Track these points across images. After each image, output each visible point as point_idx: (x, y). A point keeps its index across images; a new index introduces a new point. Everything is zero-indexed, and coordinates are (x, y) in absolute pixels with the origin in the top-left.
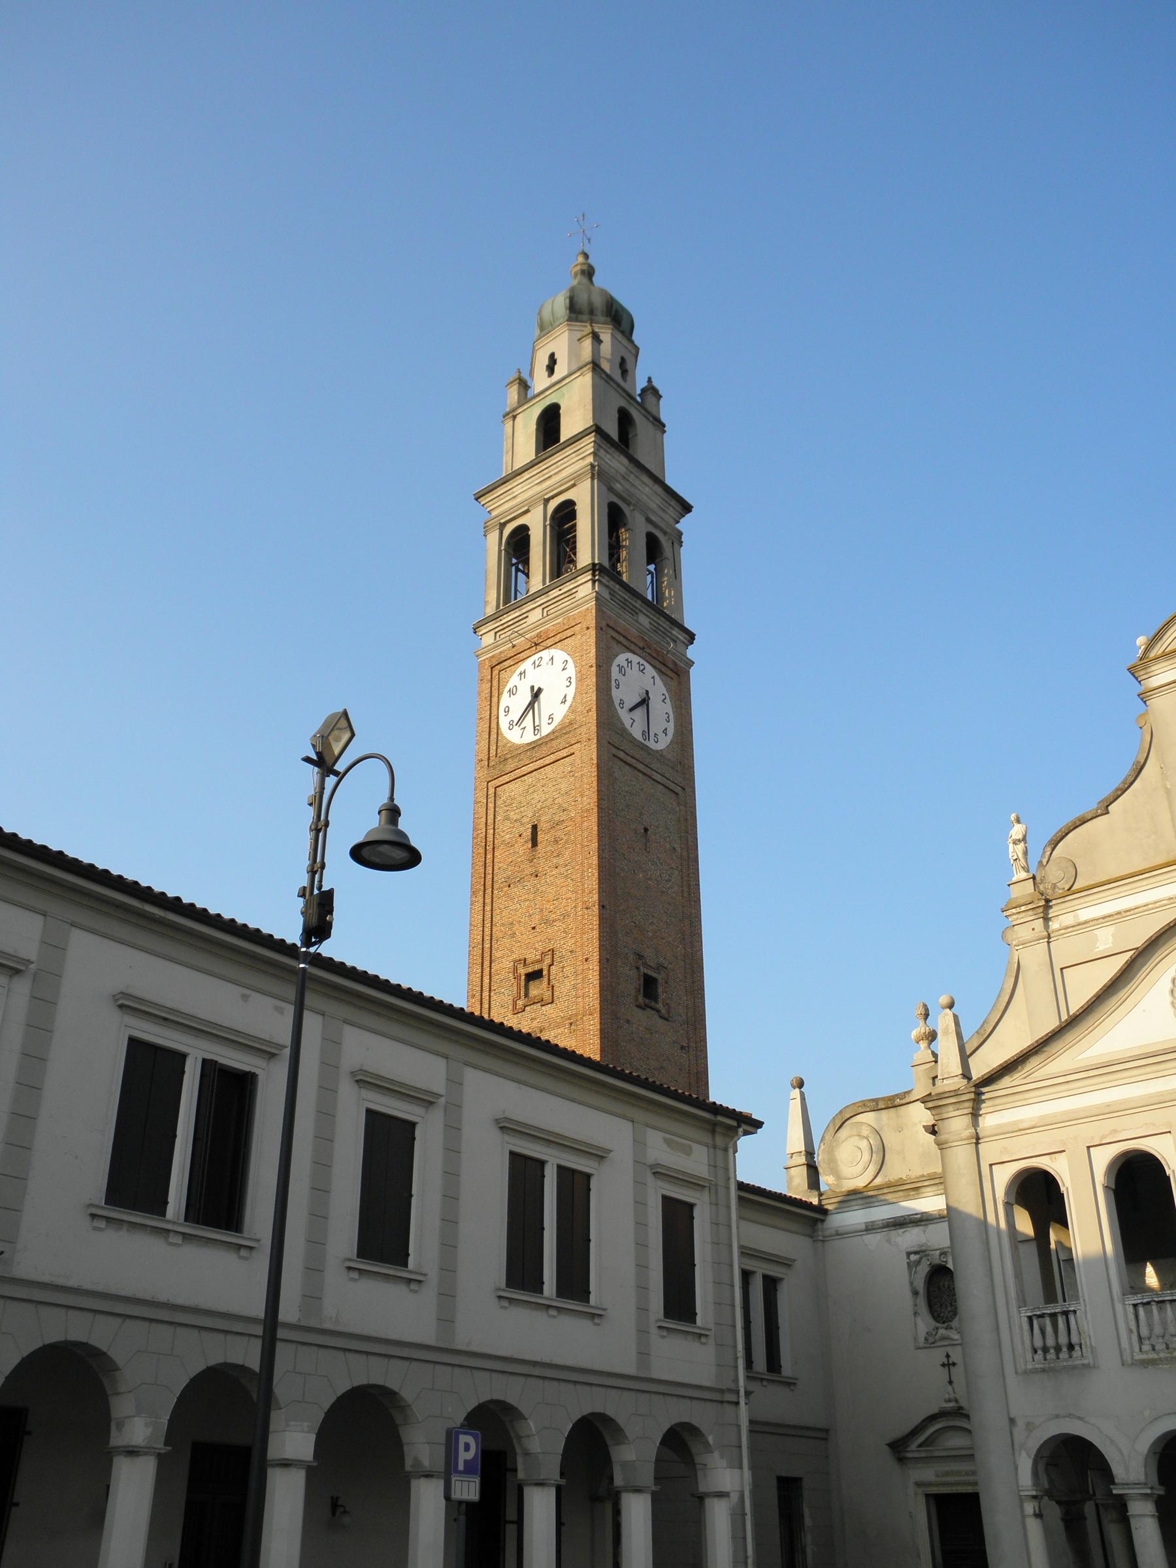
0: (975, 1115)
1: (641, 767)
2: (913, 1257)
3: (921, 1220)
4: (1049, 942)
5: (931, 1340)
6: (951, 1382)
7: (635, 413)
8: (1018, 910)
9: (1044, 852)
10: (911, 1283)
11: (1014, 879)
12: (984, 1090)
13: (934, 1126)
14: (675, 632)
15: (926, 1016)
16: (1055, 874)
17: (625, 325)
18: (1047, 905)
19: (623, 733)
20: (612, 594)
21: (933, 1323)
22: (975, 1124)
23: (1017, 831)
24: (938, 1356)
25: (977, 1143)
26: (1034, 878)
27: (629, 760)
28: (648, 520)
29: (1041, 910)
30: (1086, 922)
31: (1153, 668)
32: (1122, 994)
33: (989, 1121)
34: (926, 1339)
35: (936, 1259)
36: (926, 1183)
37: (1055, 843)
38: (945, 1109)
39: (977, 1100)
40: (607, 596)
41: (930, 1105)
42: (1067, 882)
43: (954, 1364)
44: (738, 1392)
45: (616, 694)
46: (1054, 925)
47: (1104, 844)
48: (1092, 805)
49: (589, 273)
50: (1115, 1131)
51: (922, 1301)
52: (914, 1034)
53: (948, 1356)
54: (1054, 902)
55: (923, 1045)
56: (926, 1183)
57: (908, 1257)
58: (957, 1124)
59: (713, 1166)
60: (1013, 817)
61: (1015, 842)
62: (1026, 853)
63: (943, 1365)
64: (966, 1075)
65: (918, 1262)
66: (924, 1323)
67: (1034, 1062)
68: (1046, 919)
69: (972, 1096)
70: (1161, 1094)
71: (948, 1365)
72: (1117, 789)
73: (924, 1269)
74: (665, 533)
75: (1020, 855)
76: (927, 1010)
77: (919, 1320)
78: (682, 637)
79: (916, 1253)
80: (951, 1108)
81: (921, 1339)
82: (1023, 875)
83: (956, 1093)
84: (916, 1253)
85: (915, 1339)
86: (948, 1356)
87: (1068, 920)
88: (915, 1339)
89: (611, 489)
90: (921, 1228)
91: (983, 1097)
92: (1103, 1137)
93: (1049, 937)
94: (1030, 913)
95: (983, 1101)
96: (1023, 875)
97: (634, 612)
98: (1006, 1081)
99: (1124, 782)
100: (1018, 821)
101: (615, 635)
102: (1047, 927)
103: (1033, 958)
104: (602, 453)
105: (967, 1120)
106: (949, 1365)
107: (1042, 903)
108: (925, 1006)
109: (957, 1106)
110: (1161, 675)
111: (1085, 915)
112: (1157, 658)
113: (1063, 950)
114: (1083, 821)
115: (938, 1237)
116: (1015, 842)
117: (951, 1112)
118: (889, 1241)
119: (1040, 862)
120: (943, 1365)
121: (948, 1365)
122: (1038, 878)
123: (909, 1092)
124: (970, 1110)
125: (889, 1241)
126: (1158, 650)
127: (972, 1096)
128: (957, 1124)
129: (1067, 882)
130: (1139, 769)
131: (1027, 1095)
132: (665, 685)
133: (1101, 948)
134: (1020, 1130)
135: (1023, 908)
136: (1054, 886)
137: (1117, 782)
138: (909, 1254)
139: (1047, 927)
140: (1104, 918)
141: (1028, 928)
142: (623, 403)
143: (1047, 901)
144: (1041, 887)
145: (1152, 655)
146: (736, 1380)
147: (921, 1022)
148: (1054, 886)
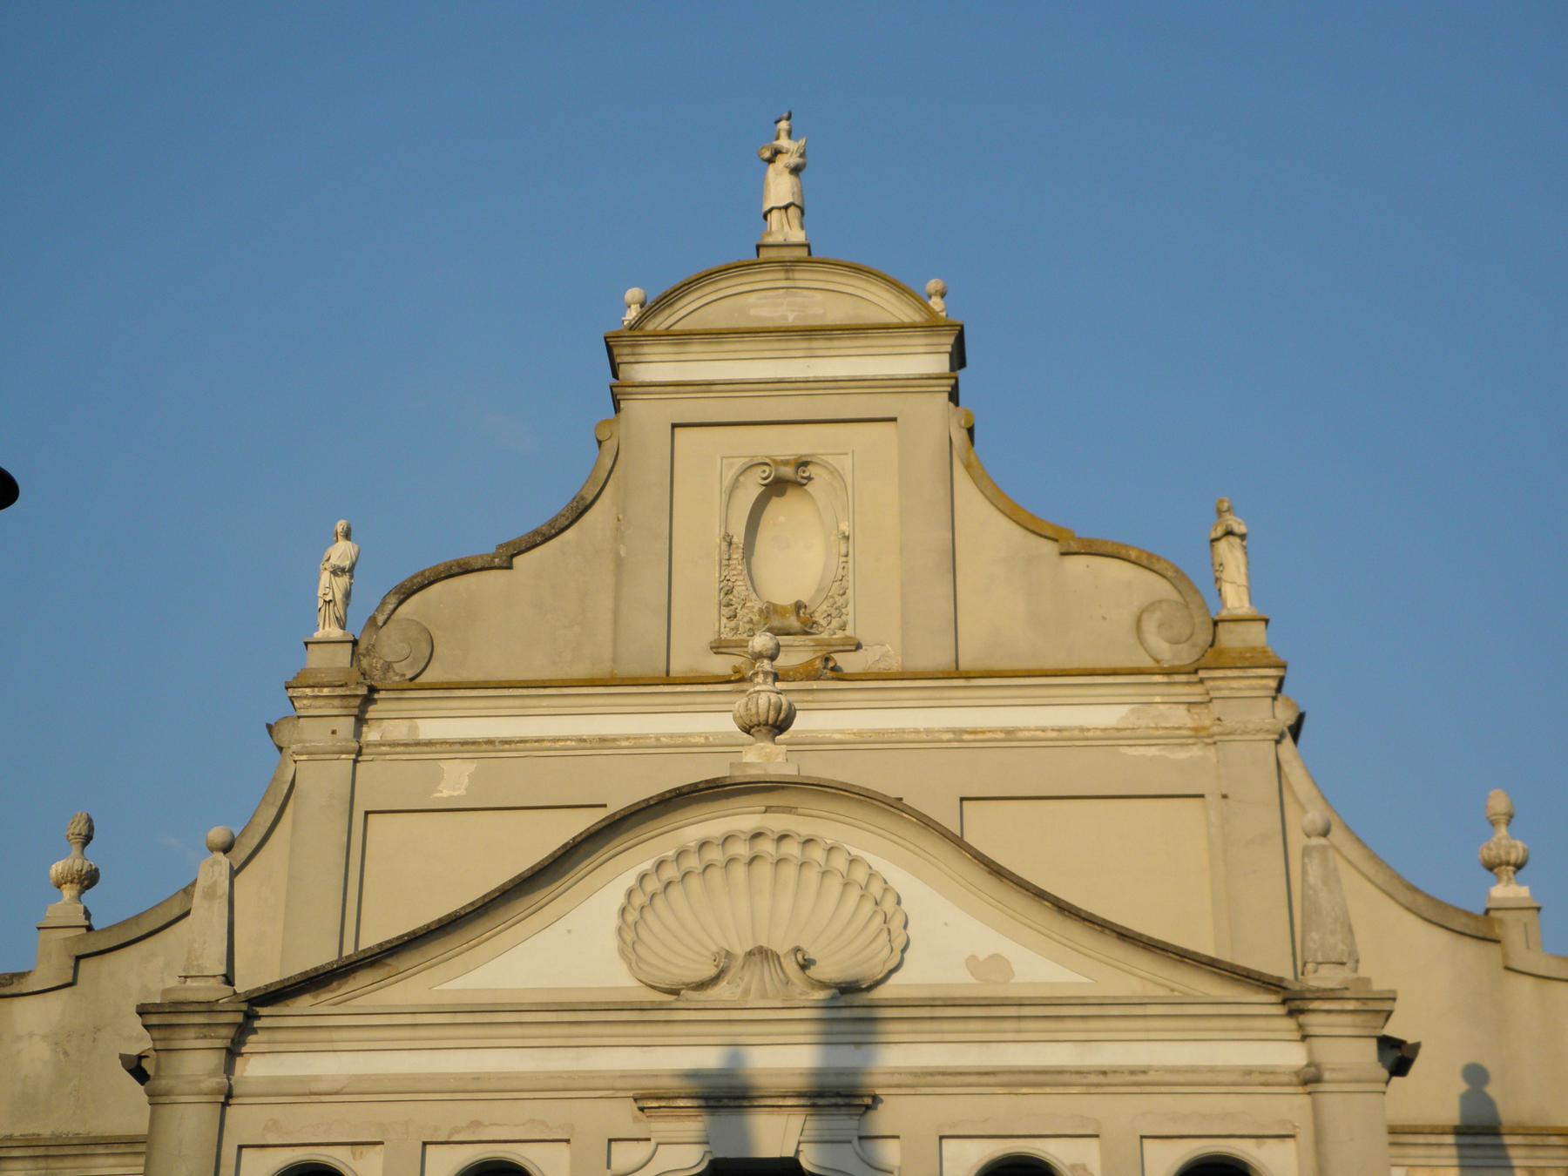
0: (233, 1053)
4: (356, 761)
8: (316, 692)
9: (383, 603)
11: (318, 635)
12: (262, 1011)
13: (140, 1057)
15: (88, 839)
16: (392, 646)
18: (368, 700)
22: (229, 1069)
23: (341, 553)
25: (225, 1104)
26: (355, 643)
29: (357, 702)
30: (429, 743)
31: (646, 350)
32: (541, 895)
33: (255, 1068)
36: (16, 1153)
37: (406, 592)
38: (178, 1033)
39: (244, 1029)
41: (154, 1020)
42: (411, 666)
46: (371, 734)
47: (491, 618)
48: (485, 547)
50: (477, 1124)
52: (57, 868)
54: (383, 694)
55: (68, 892)
56: (16, 1153)
58: (196, 1063)
60: (340, 526)
61: (337, 571)
62: (347, 595)
64: (229, 979)
67: (363, 978)
68: (361, 720)
69: (239, 1018)
70: (570, 1075)
72: (537, 532)
75: (339, 596)
76: (91, 829)
80: (192, 1033)
82: (335, 632)
83: (210, 1007)
87: (398, 730)
91: (257, 1024)
92: (456, 1130)
93: (359, 752)
94: (336, 702)
95: (255, 1031)
96: (335, 632)
98: (304, 1003)
99: (551, 524)
100: (347, 536)
102: (358, 734)
103: (321, 782)
105: (215, 1060)
107: (363, 691)
108: (89, 821)
109: (205, 1031)
110: (655, 366)
111: (430, 729)
112: (657, 336)
113: (380, 781)
114: (464, 569)
116: (337, 571)
117: (190, 1040)
119: (373, 619)
122: (362, 646)
123: (21, 976)
124: (227, 1043)
126: (659, 323)
127: (239, 1018)
128: (196, 1063)
129: (411, 666)
130: (579, 510)
131: (336, 1035)
133: (446, 793)
134: (308, 1093)
135: (326, 691)
136: (388, 666)
137: (538, 519)
139: (358, 734)
140: (464, 743)
141: (324, 726)
143: (373, 690)
144: (365, 663)
145: (650, 326)
147: (75, 850)
148: (388, 666)
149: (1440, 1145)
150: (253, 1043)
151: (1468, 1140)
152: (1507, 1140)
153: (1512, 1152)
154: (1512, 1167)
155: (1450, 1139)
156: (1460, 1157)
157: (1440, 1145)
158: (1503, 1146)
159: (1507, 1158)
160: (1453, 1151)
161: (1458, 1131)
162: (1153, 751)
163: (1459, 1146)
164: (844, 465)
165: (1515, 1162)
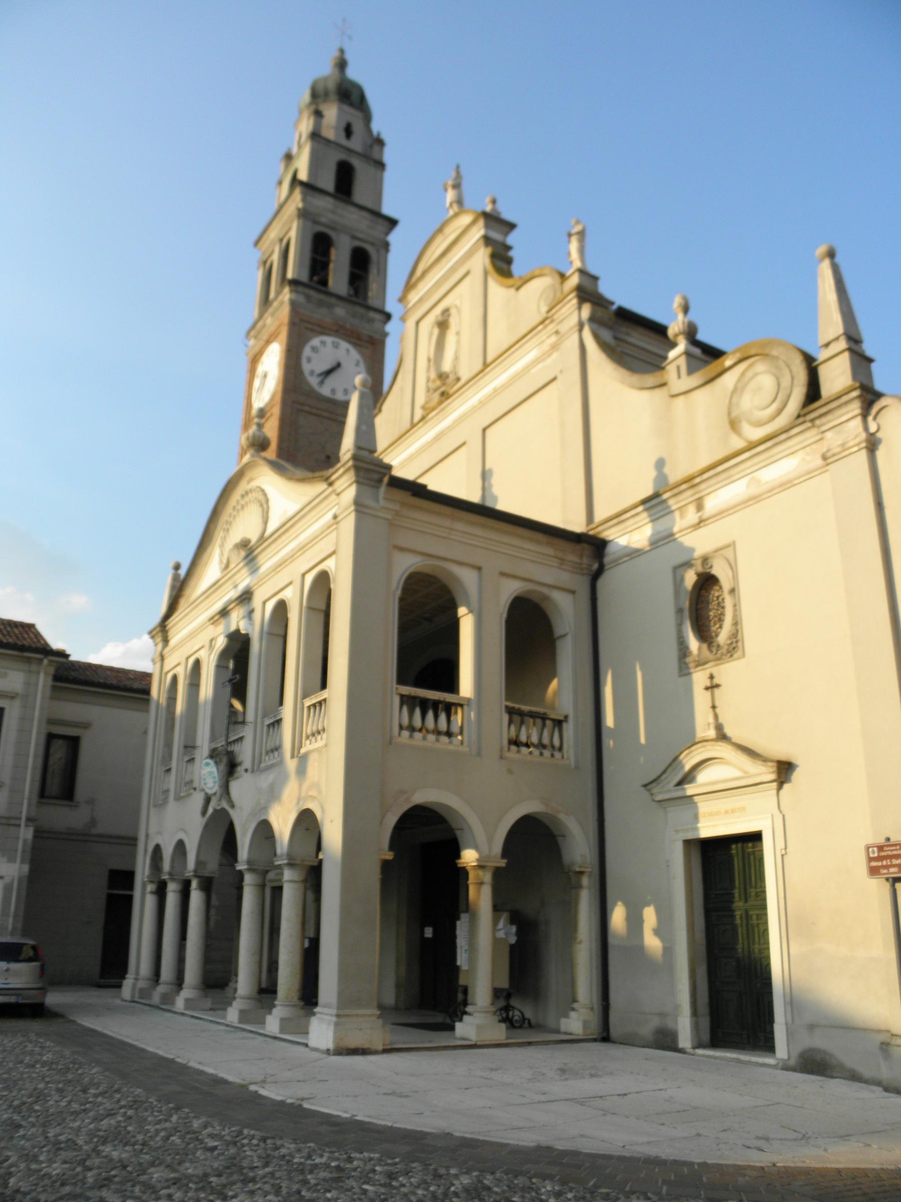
1: (326, 414)
7: (356, 162)
14: (372, 314)
17: (355, 97)
19: (312, 394)
20: (308, 298)
27: (314, 411)
28: (354, 237)
40: (301, 299)
44: (20, 819)
45: (306, 367)
49: (342, 64)
59: (27, 684)
74: (373, 244)
78: (378, 316)
89: (316, 222)
97: (330, 306)
101: (310, 326)
104: (309, 198)
132: (361, 353)
142: (342, 156)
146: (21, 812)
149: (637, 514)
150: (171, 634)
151: (648, 505)
152: (665, 496)
153: (671, 502)
154: (672, 512)
155: (641, 508)
156: (650, 516)
157: (637, 514)
158: (665, 501)
159: (669, 507)
160: (645, 515)
161: (644, 502)
162: (540, 366)
163: (646, 510)
164: (458, 303)
165: (674, 508)
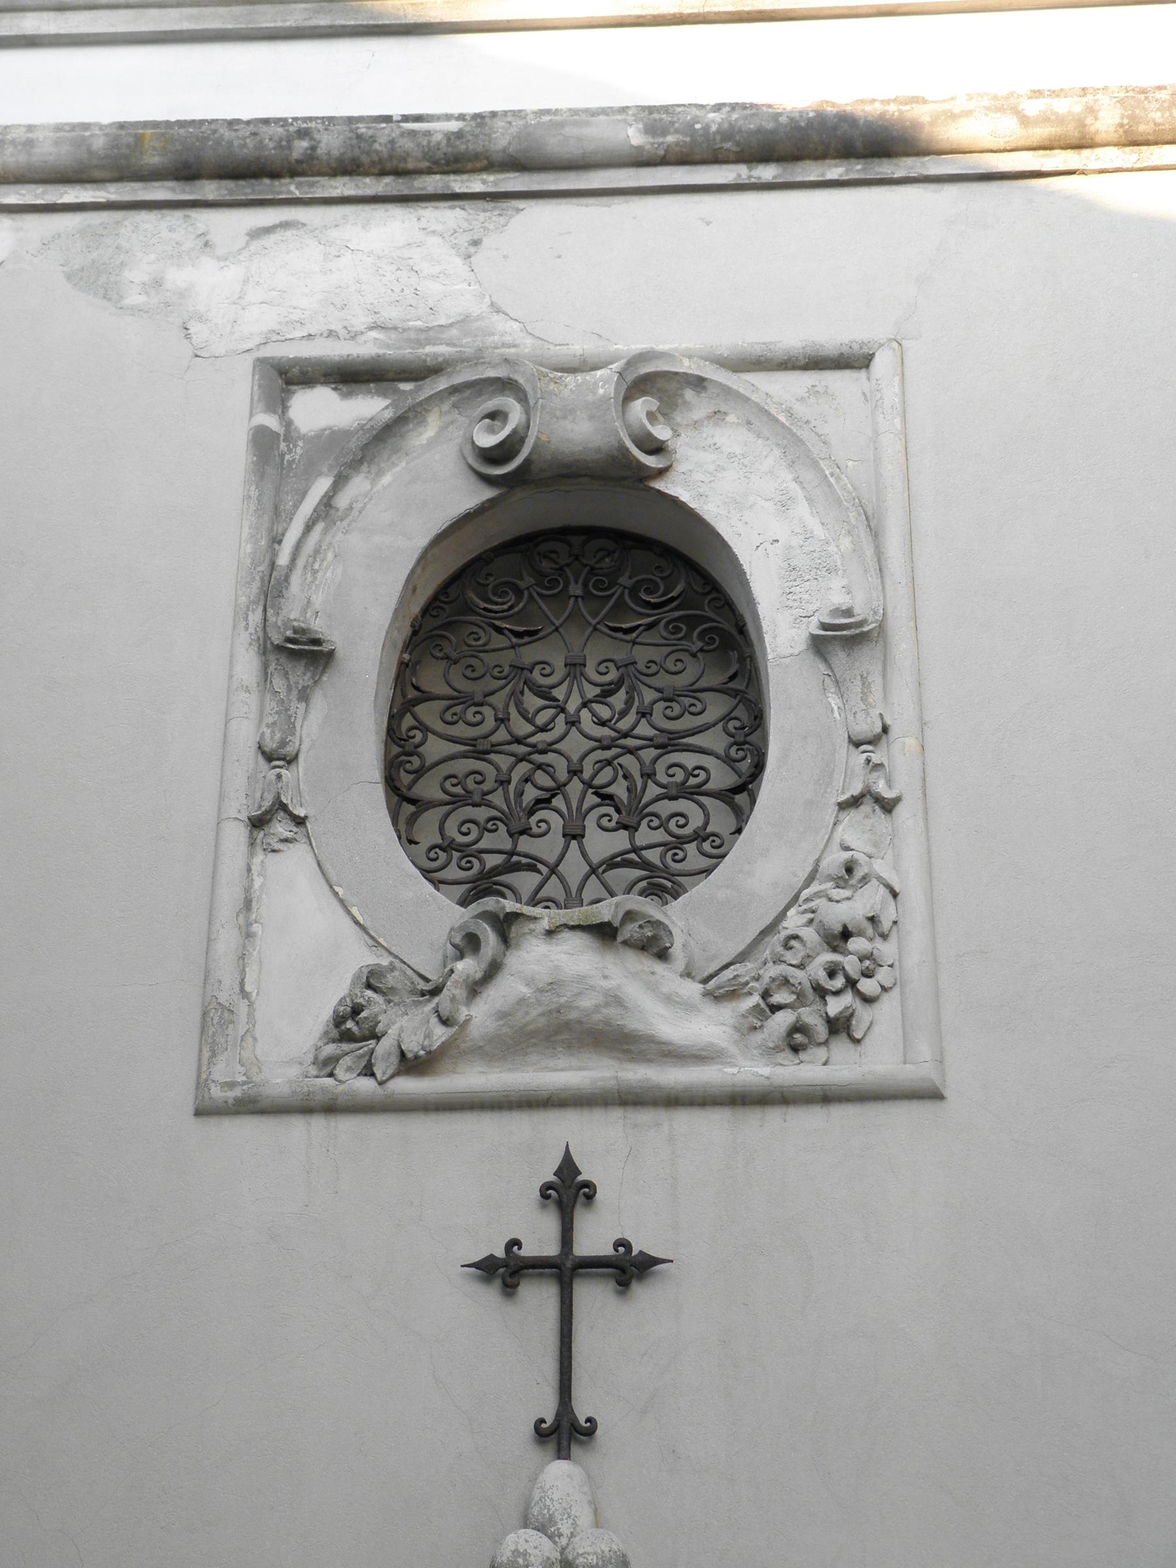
2: (319, 410)
3: (455, 160)
5: (409, 1027)
6: (564, 1433)
10: (272, 588)
21: (445, 913)
24: (484, 1185)
34: (351, 1027)
35: (576, 423)
43: (628, 1268)
51: (346, 727)
53: (568, 1191)
57: (277, 401)
63: (505, 1271)
65: (382, 438)
66: (340, 908)
71: (564, 1266)
73: (425, 492)
77: (290, 880)
79: (349, 376)
81: (286, 1038)
84: (349, 376)
85: (216, 1022)
86: (568, 1191)
88: (216, 1022)
90: (447, 217)
106: (565, 1270)
115: (571, 297)
118: (96, 280)
120: (505, 1271)
121: (564, 1266)
125: (96, 280)
138: (287, 377)
